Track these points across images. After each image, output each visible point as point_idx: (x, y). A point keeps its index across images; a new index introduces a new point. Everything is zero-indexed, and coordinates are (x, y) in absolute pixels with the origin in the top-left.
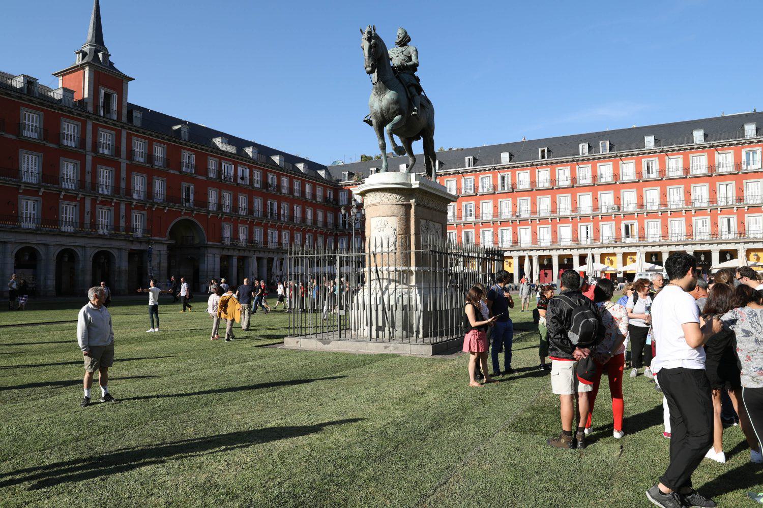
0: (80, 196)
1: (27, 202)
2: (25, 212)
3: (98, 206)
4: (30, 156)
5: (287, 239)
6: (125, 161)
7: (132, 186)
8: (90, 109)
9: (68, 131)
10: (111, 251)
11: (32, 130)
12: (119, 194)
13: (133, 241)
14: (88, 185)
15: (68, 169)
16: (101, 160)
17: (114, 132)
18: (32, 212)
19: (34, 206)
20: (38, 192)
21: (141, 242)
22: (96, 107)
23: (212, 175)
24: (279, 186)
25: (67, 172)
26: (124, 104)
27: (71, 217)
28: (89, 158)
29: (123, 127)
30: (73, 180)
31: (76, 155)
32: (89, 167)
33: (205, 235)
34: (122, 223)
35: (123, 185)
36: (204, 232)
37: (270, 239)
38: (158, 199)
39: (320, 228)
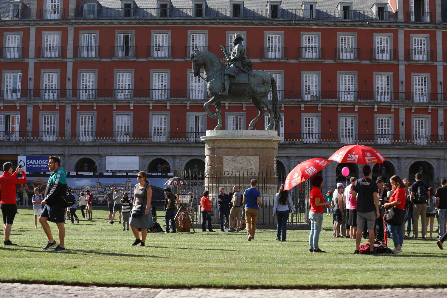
0: (393, 107)
2: (344, 128)
6: (441, 63)
8: (401, 17)
9: (381, 44)
10: (429, 162)
14: (402, 96)
15: (382, 82)
18: (351, 128)
19: (352, 122)
22: (407, 14)
25: (382, 85)
27: (387, 129)
28: (402, 68)
29: (437, 28)
30: (388, 92)
32: (402, 77)
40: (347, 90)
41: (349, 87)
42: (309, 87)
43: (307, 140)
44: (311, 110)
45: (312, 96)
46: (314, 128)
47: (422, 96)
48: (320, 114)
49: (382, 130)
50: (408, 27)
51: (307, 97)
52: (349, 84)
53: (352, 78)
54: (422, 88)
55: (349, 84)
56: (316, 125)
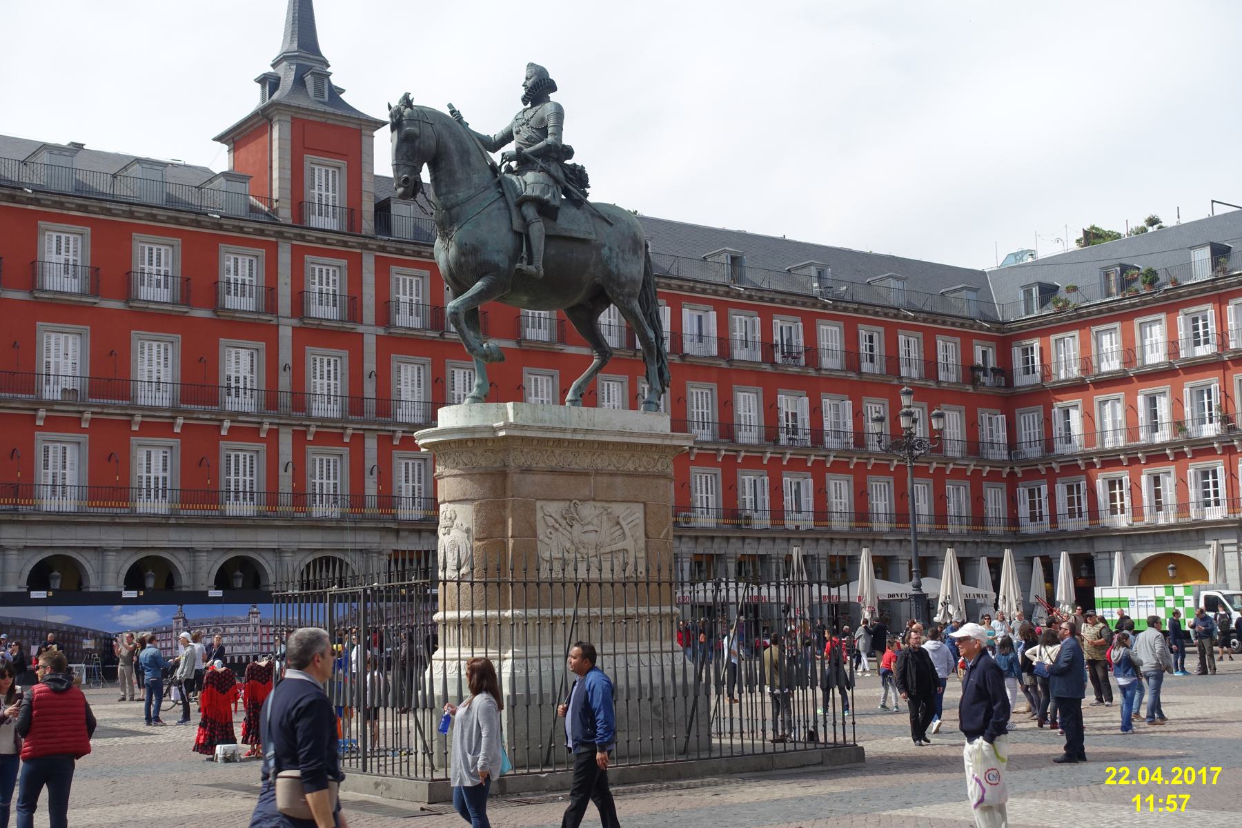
0: (266, 427)
1: (149, 454)
2: (145, 475)
3: (310, 449)
4: (155, 345)
5: (845, 500)
6: (373, 329)
7: (394, 391)
9: (236, 273)
11: (158, 281)
15: (239, 364)
16: (313, 335)
17: (344, 262)
18: (161, 475)
19: (165, 459)
20: (172, 425)
21: (419, 531)
24: (812, 352)
25: (237, 371)
26: (367, 186)
28: (285, 333)
29: (365, 247)
31: (255, 328)
35: (370, 389)
37: (788, 499)
39: (953, 459)
40: (155, 380)
41: (159, 371)
42: (57, 364)
43: (49, 503)
44: (62, 422)
45: (64, 390)
46: (68, 471)
47: (329, 402)
49: (237, 481)
50: (303, 238)
51: (52, 392)
52: (159, 364)
53: (166, 350)
54: (329, 385)
55: (159, 364)
56: (72, 464)
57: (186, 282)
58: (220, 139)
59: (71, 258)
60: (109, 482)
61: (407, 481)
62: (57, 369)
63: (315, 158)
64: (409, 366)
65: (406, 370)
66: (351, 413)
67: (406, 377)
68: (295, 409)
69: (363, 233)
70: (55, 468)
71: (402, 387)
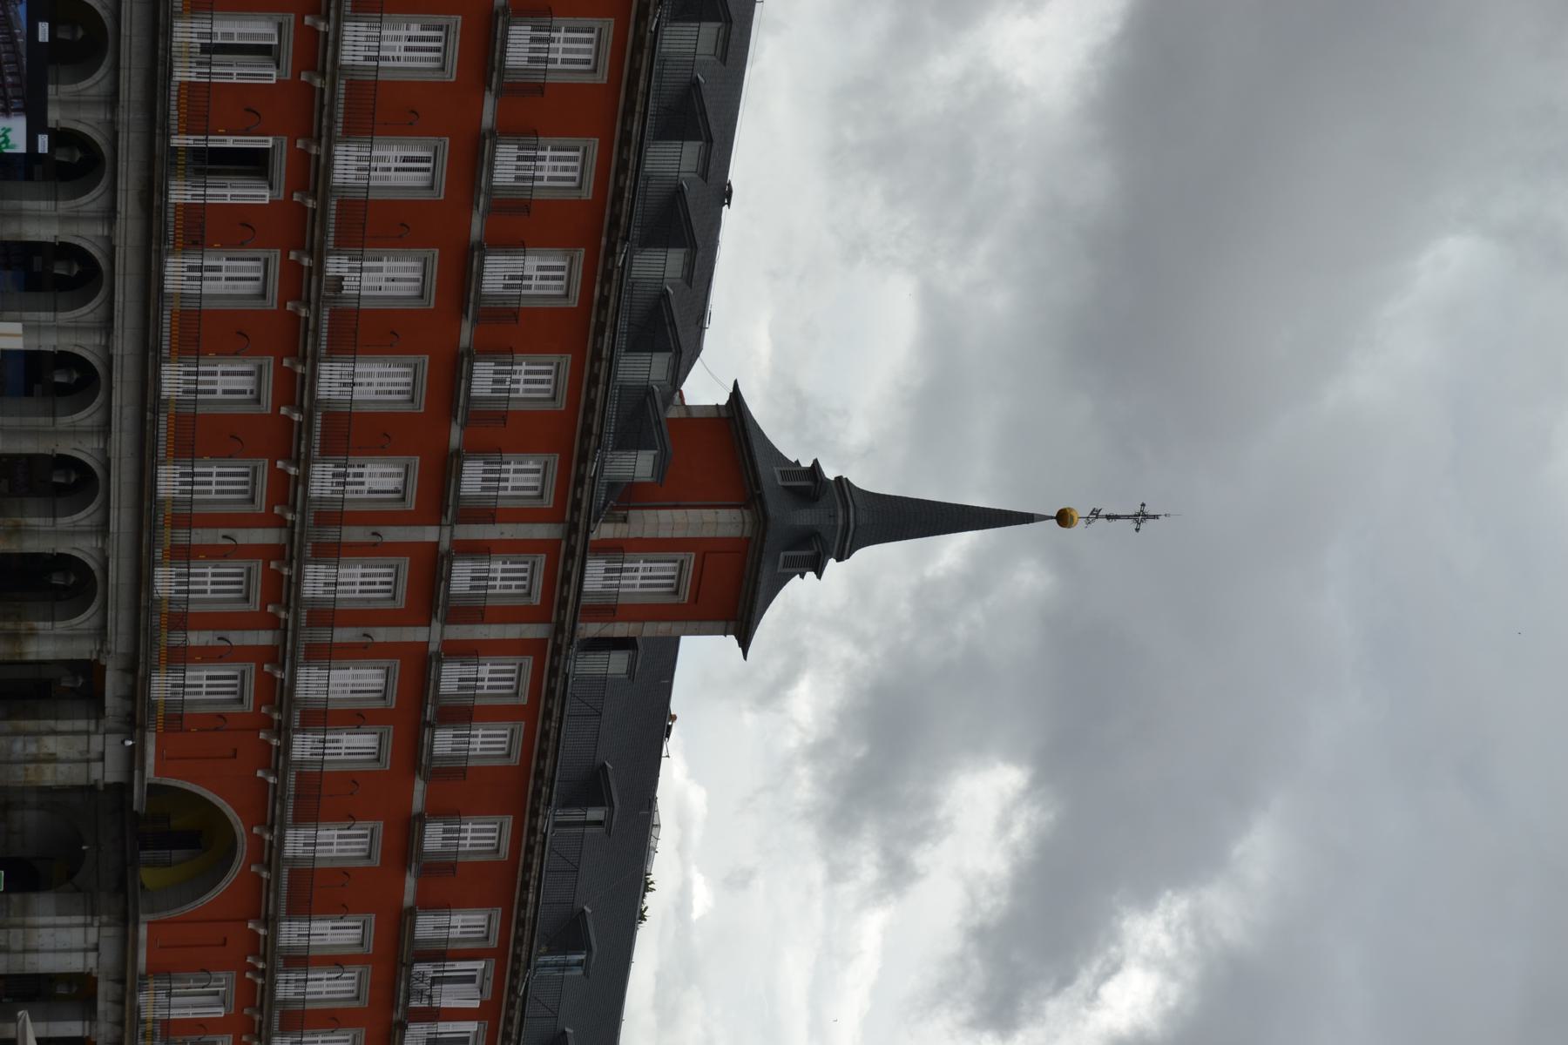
7: (345, 663)
11: (503, 382)
12: (310, 624)
13: (136, 671)
14: (331, 534)
18: (219, 388)
19: (244, 392)
20: (290, 403)
23: (427, 927)
25: (371, 475)
26: (651, 629)
28: (430, 534)
33: (175, 913)
34: (196, 638)
35: (344, 635)
36: (188, 908)
38: (303, 746)
40: (357, 380)
41: (369, 384)
45: (342, 278)
46: (223, 283)
48: (271, 303)
51: (336, 265)
55: (381, 384)
57: (502, 417)
58: (736, 395)
59: (533, 283)
60: (203, 435)
61: (209, 678)
62: (370, 270)
63: (690, 566)
64: (382, 681)
65: (377, 676)
66: (311, 613)
67: (366, 676)
68: (316, 546)
69: (580, 625)
70: (228, 269)
71: (351, 671)
